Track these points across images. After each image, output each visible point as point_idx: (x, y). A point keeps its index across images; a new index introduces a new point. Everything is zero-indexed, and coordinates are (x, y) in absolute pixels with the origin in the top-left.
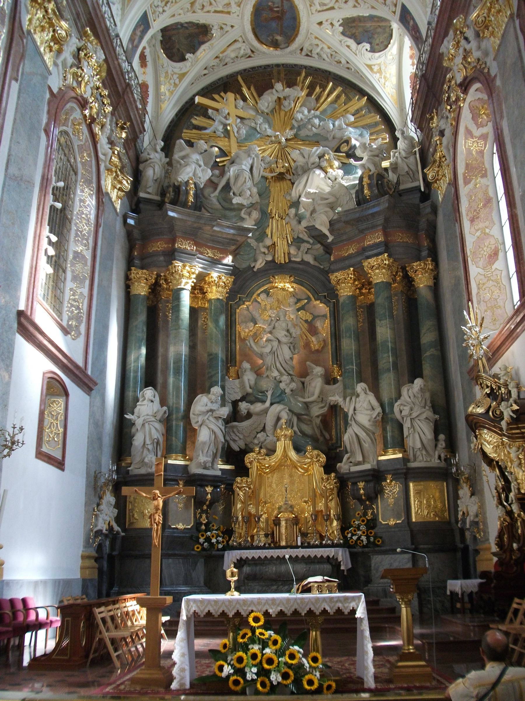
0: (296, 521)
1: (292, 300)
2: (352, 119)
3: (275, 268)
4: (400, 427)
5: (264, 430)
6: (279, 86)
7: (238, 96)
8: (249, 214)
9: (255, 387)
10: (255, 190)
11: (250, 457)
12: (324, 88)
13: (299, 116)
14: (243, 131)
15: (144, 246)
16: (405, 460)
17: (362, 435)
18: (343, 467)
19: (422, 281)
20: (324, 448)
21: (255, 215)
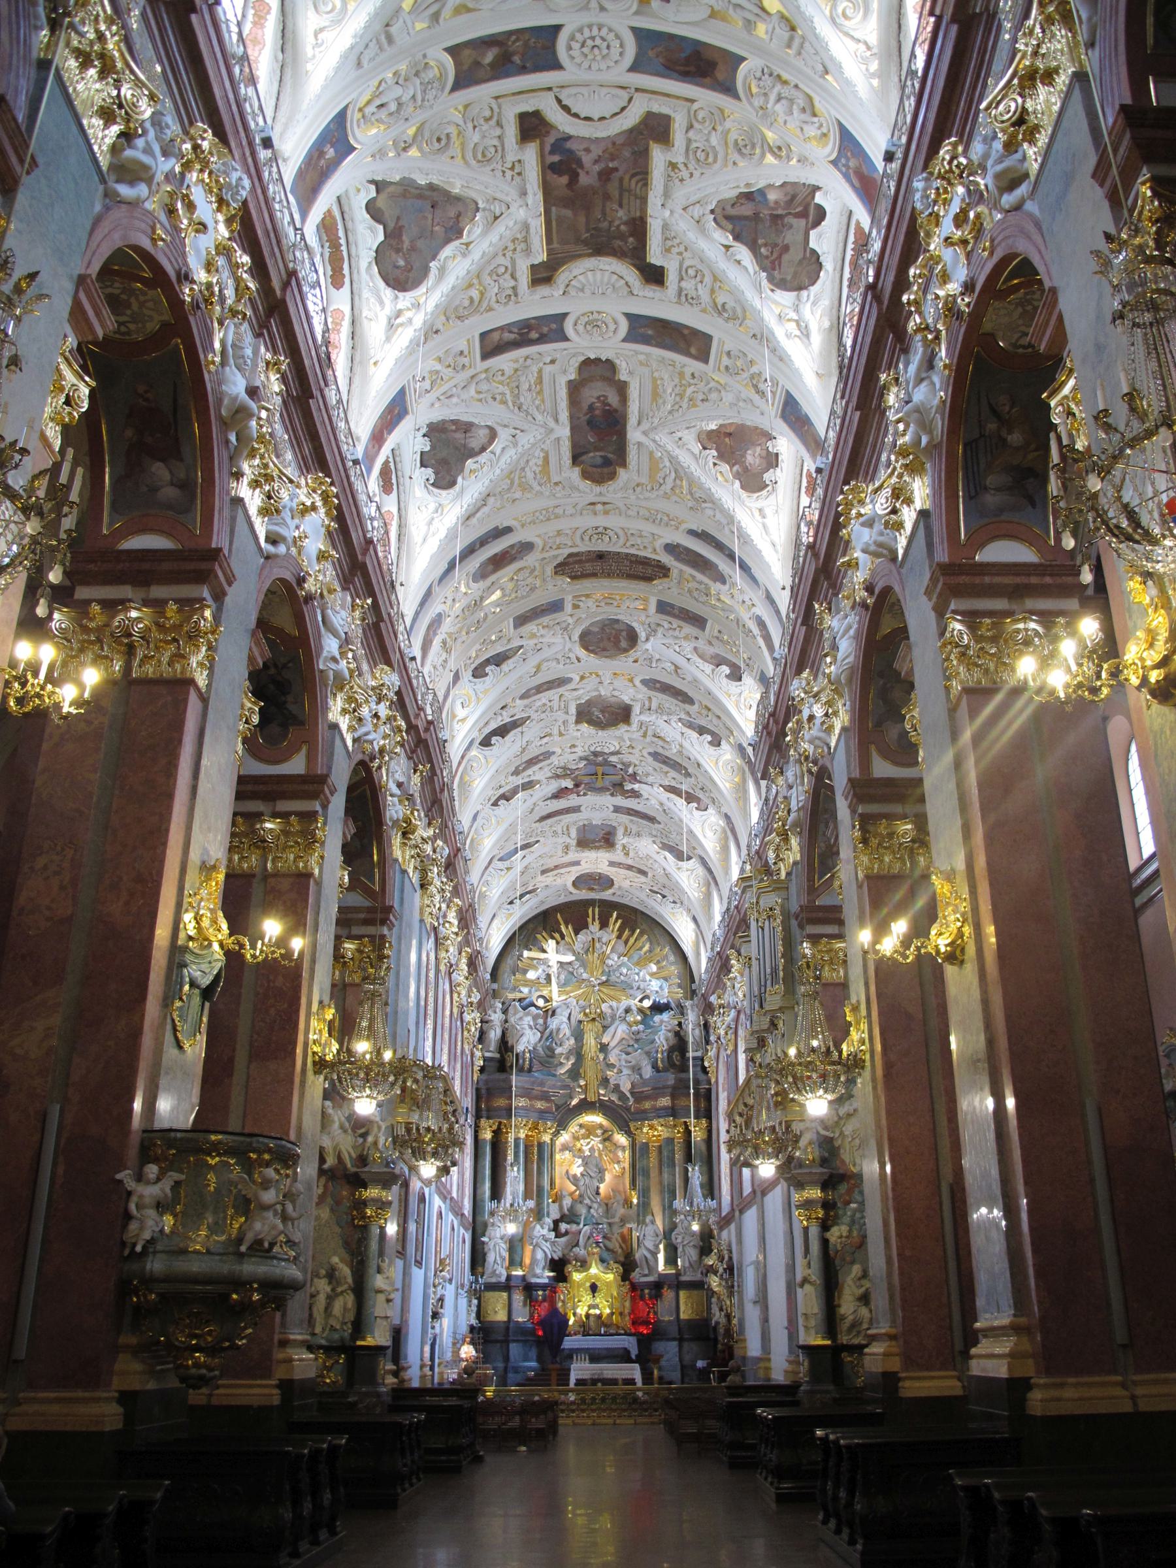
0: (600, 1316)
1: (599, 1132)
2: (654, 968)
3: (586, 1106)
4: (676, 1249)
5: (577, 1245)
6: (594, 927)
7: (557, 935)
8: (568, 1059)
9: (571, 1209)
10: (572, 1041)
11: (569, 1268)
12: (633, 932)
13: (610, 962)
14: (563, 977)
15: (488, 1101)
16: (678, 1274)
17: (649, 1256)
18: (636, 1276)
19: (698, 1135)
20: (622, 1259)
21: (572, 1061)
